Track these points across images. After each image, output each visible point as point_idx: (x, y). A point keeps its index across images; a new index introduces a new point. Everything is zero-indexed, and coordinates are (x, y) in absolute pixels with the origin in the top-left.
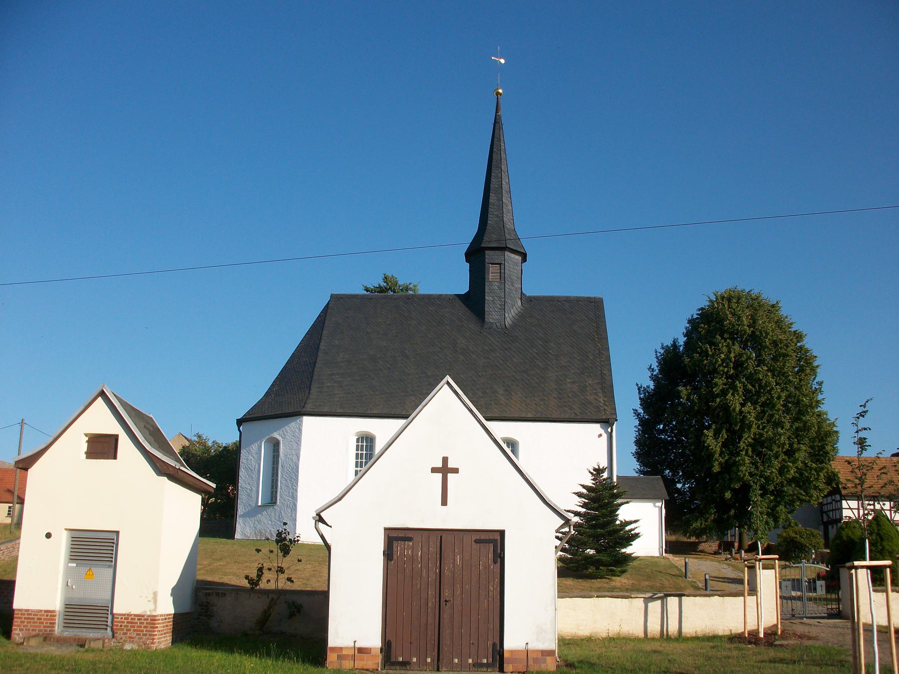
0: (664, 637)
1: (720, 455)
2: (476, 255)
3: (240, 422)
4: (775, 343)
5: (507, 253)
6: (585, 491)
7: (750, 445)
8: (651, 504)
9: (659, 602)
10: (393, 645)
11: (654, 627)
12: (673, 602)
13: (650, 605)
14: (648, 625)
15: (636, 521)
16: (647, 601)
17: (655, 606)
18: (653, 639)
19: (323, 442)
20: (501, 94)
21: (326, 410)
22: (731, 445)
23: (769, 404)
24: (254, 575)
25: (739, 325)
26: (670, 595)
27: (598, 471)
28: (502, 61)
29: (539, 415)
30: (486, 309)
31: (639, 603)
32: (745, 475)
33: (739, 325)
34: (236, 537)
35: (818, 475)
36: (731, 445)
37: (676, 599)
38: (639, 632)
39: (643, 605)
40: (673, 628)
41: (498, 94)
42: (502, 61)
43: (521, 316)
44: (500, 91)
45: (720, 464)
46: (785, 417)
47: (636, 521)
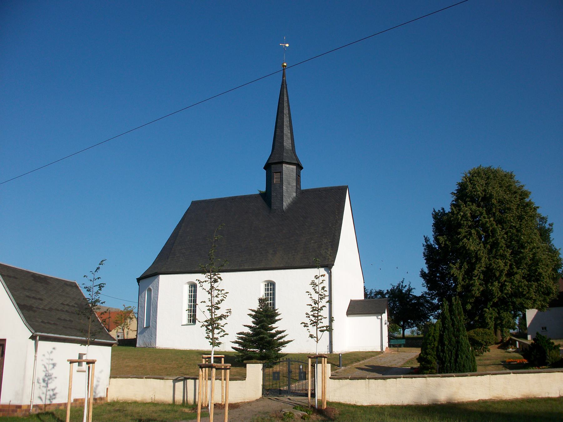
0: (185, 404)
1: (463, 280)
2: (272, 167)
3: (139, 280)
4: (500, 202)
5: (284, 165)
6: (254, 313)
7: (483, 272)
8: (375, 317)
9: (182, 382)
10: (238, 410)
11: (179, 397)
12: (190, 383)
13: (177, 384)
14: (176, 396)
15: (283, 331)
16: (175, 381)
17: (180, 385)
18: (178, 405)
19: (173, 289)
20: (285, 66)
21: (171, 270)
22: (469, 274)
23: (495, 245)
24: (45, 370)
25: (474, 192)
26: (189, 378)
27: (261, 301)
28: (287, 45)
29: (287, 265)
30: (272, 201)
31: (170, 382)
32: (475, 293)
33: (474, 192)
34: (137, 345)
35: (529, 290)
36: (469, 274)
37: (193, 381)
38: (169, 399)
39: (172, 384)
40: (190, 398)
41: (284, 66)
42: (287, 45)
43: (295, 203)
44: (285, 64)
45: (463, 286)
46: (507, 251)
47: (283, 331)
